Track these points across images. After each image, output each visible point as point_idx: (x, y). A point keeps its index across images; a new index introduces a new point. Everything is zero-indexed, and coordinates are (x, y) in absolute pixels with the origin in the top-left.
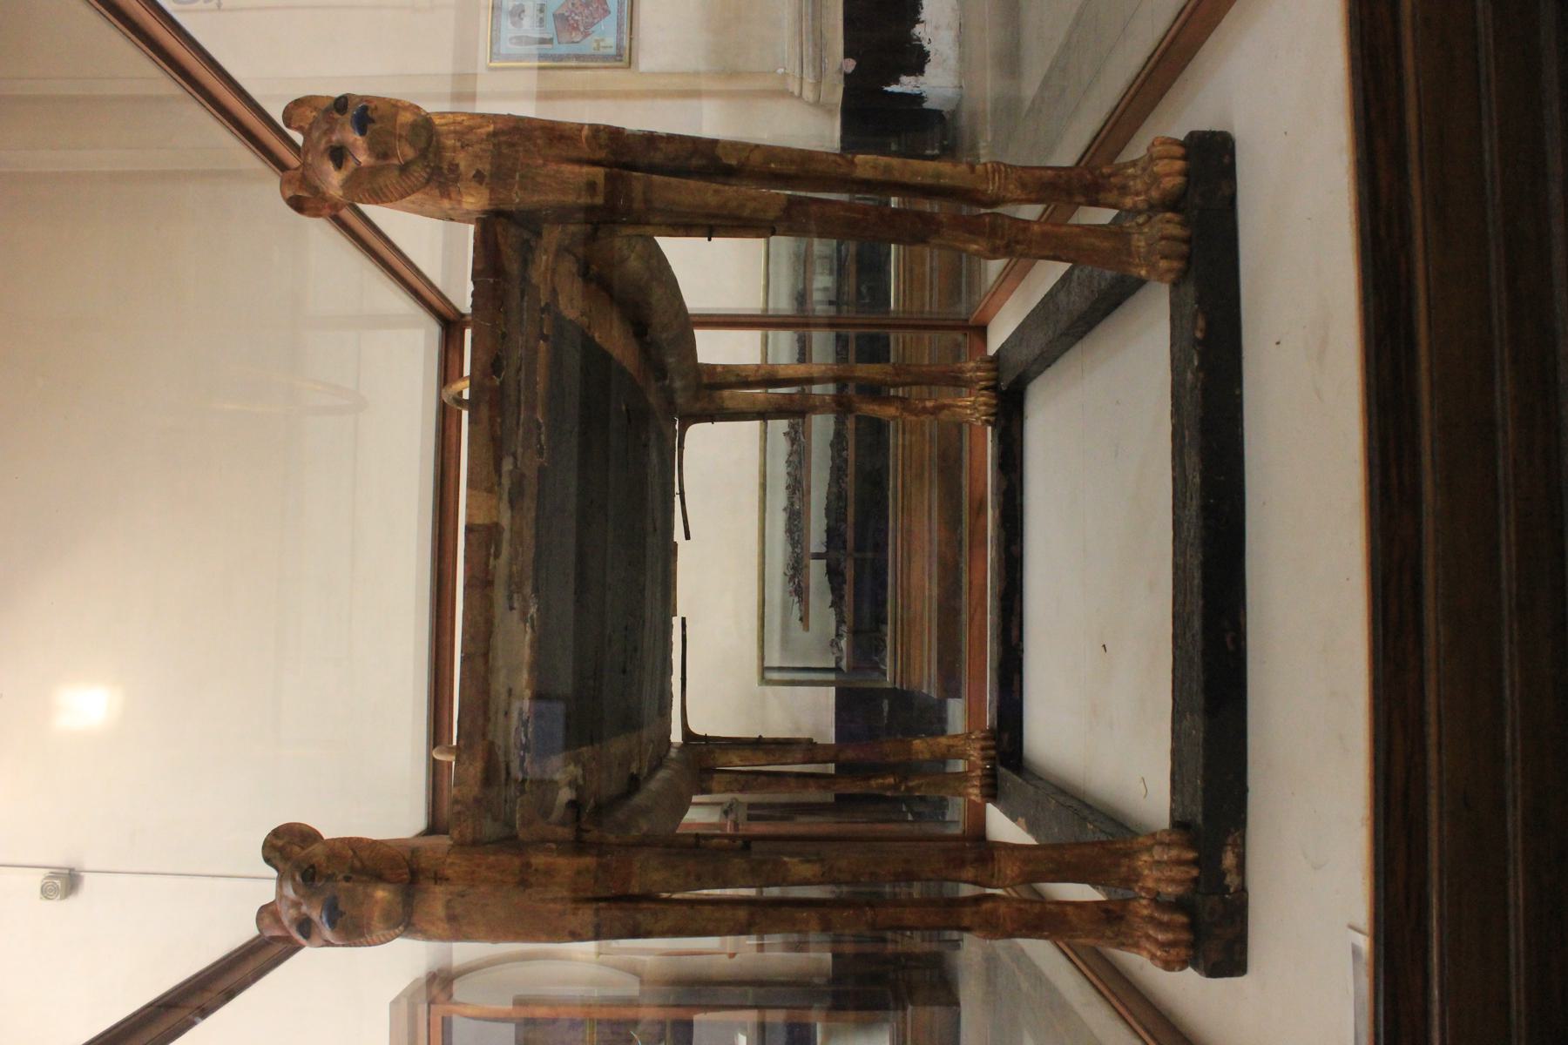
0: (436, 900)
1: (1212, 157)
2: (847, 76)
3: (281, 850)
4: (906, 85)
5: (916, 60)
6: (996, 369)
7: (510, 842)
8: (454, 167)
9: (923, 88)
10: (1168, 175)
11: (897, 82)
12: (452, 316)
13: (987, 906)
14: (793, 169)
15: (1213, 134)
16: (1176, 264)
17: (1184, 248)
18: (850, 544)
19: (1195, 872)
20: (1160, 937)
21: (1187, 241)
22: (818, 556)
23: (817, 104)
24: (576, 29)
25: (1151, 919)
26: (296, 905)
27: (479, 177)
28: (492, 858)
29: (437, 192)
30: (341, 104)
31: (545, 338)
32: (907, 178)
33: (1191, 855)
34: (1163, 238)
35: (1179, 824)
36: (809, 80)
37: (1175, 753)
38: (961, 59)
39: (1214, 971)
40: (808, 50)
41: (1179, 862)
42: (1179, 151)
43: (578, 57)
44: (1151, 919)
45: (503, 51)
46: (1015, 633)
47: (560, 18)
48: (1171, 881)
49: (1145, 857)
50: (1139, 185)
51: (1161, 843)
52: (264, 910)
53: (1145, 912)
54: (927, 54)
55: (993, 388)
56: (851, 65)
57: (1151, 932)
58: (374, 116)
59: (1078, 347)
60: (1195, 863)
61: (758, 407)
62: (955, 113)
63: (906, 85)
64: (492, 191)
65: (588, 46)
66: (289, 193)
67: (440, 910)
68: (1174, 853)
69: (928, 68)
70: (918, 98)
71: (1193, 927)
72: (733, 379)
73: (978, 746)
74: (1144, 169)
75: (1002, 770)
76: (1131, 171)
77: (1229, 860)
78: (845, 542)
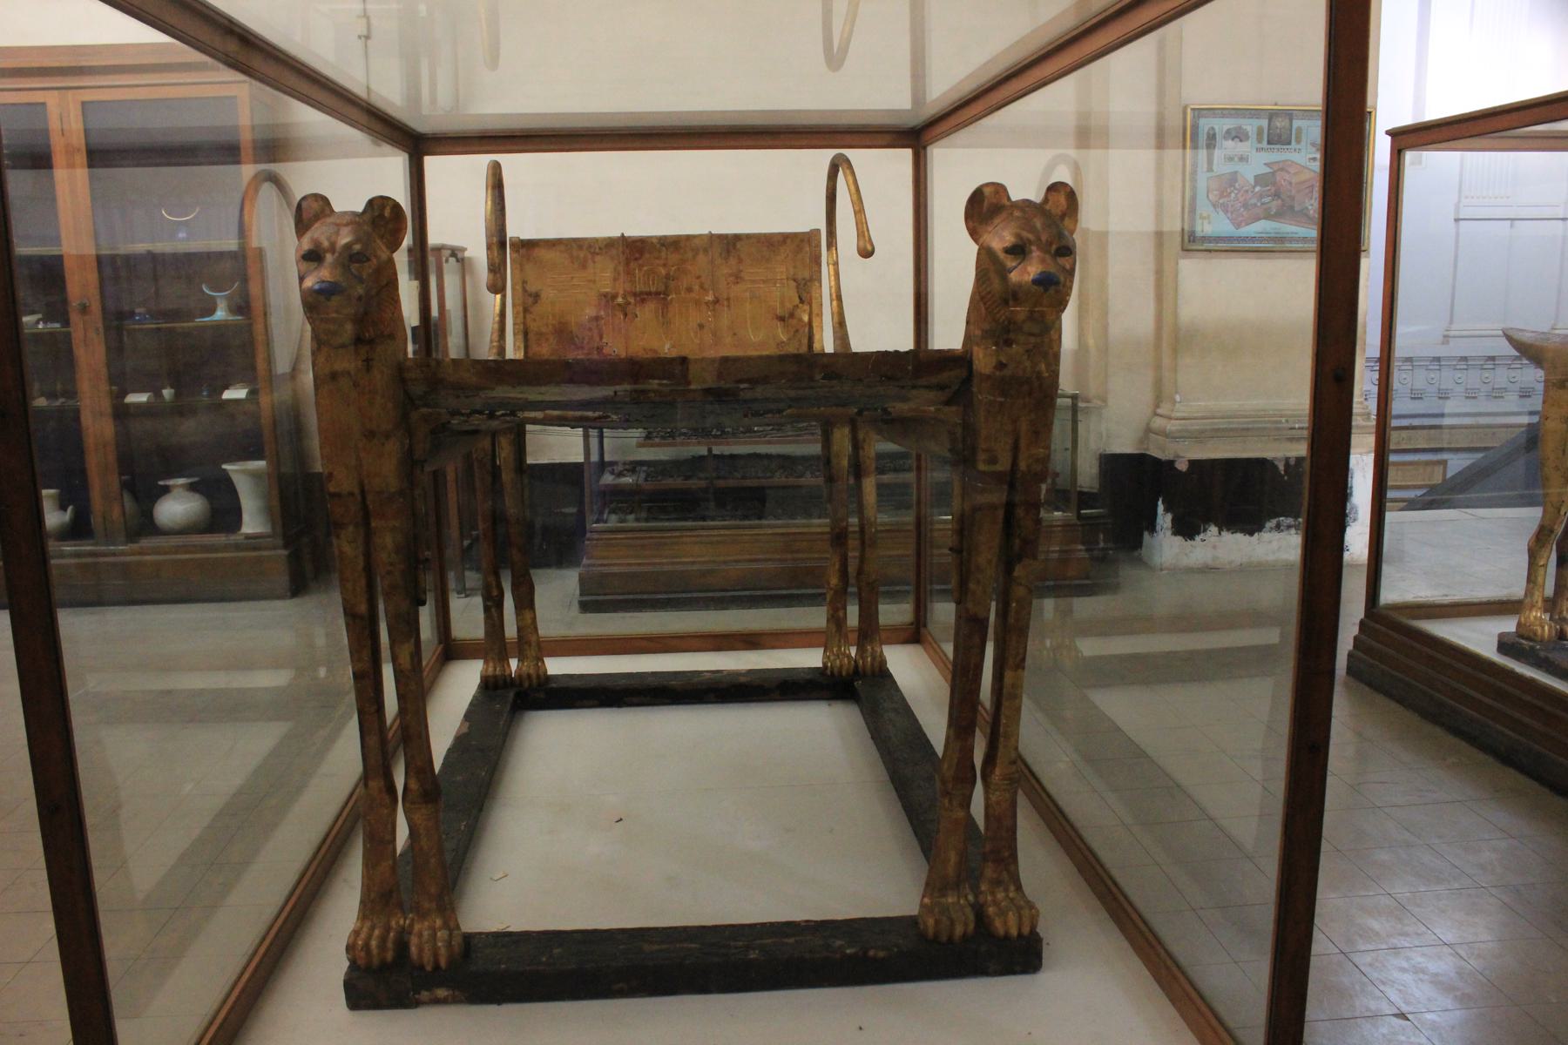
0: (347, 363)
1: (1020, 955)
2: (1171, 463)
3: (381, 216)
4: (1164, 519)
5: (1187, 528)
6: (873, 674)
7: (407, 403)
8: (1008, 343)
9: (1161, 535)
10: (1005, 923)
11: (1167, 510)
12: (927, 136)
13: (387, 800)
14: (1011, 620)
15: (1039, 956)
16: (931, 931)
17: (944, 938)
18: (721, 483)
19: (429, 968)
20: (374, 943)
21: (950, 939)
22: (710, 450)
23: (1148, 430)
24: (1222, 196)
25: (387, 929)
26: (332, 249)
27: (1001, 366)
28: (390, 405)
29: (986, 326)
30: (1066, 251)
31: (860, 413)
32: (1005, 711)
33: (443, 963)
34: (952, 923)
35: (470, 941)
36: (1171, 426)
37: (526, 936)
38: (1190, 570)
39: (349, 986)
40: (1195, 426)
41: (436, 955)
42: (1026, 931)
43: (1194, 199)
44: (387, 929)
45: (1202, 121)
46: (635, 700)
47: (1233, 178)
48: (421, 950)
49: (439, 922)
50: (1000, 895)
51: (451, 935)
52: (325, 200)
53: (393, 923)
54: (1192, 538)
55: (857, 672)
56: (1182, 466)
57: (377, 932)
58: (1052, 291)
59: (883, 774)
60: (437, 967)
61: (834, 461)
62: (1140, 562)
63: (1164, 519)
64: (988, 377)
65: (1203, 207)
66: (987, 191)
67: (339, 366)
68: (443, 951)
69: (1179, 539)
70: (1152, 528)
71: (384, 967)
72: (861, 436)
73: (532, 672)
74: (1012, 900)
75: (511, 695)
76: (1012, 888)
77: (441, 993)
78: (725, 478)
